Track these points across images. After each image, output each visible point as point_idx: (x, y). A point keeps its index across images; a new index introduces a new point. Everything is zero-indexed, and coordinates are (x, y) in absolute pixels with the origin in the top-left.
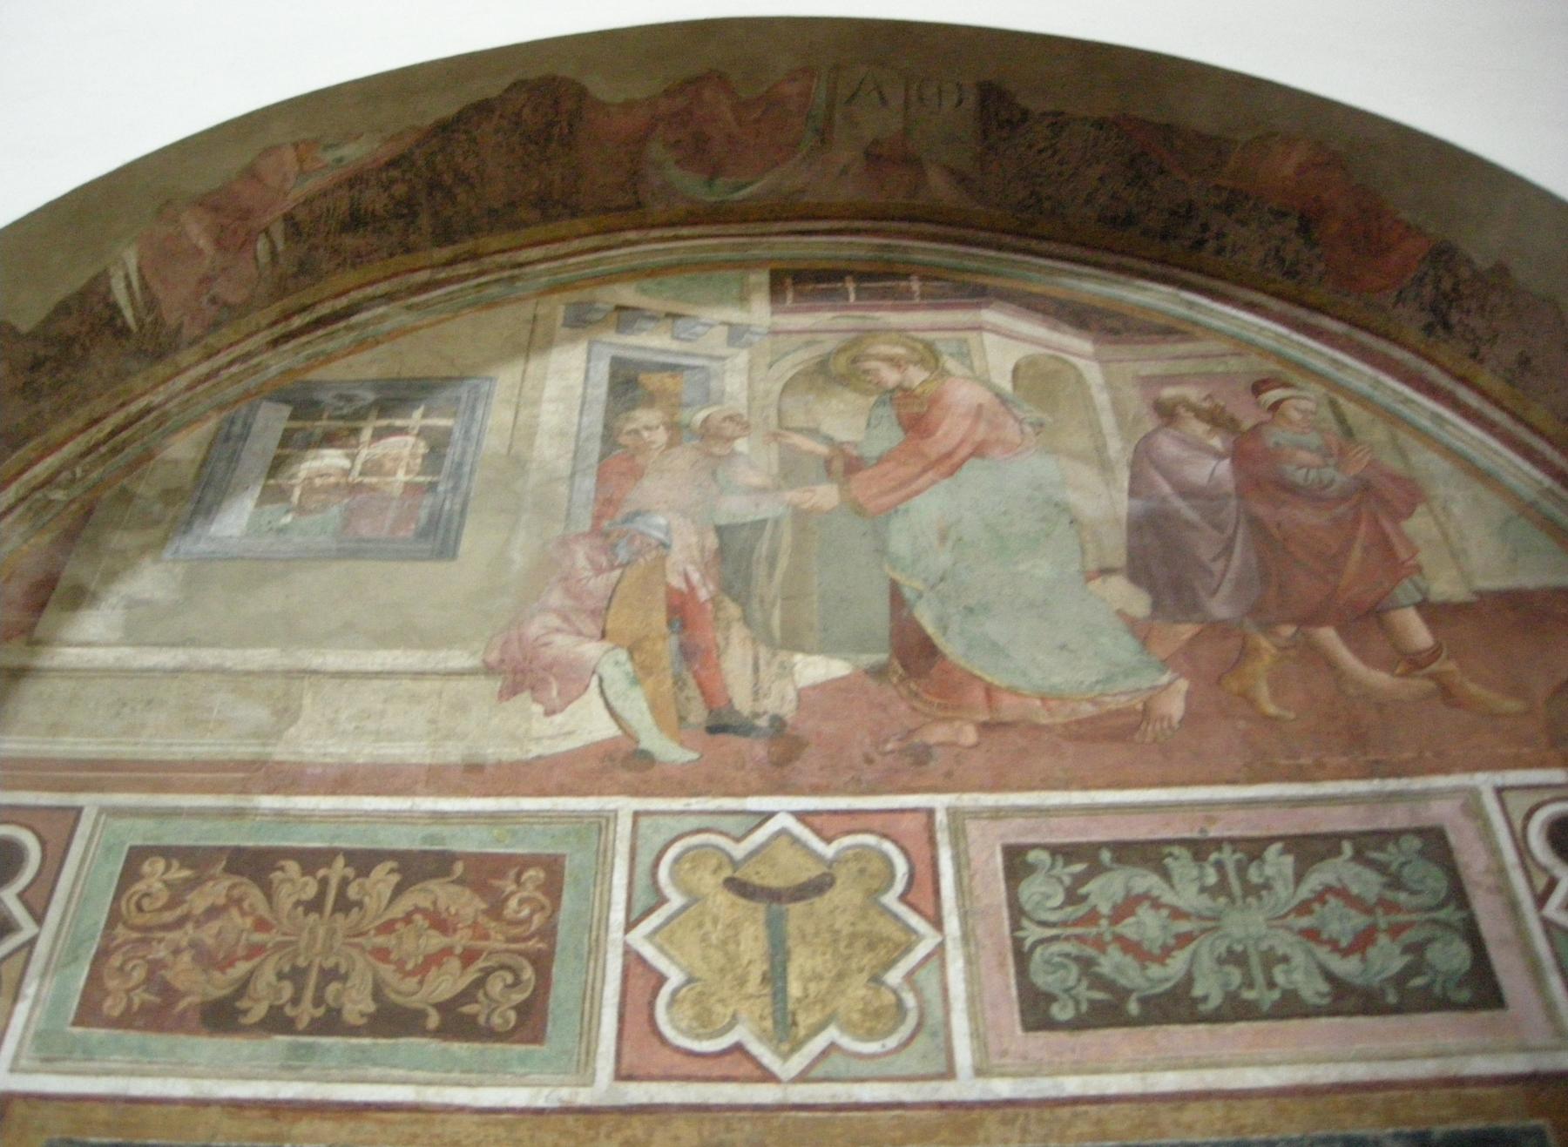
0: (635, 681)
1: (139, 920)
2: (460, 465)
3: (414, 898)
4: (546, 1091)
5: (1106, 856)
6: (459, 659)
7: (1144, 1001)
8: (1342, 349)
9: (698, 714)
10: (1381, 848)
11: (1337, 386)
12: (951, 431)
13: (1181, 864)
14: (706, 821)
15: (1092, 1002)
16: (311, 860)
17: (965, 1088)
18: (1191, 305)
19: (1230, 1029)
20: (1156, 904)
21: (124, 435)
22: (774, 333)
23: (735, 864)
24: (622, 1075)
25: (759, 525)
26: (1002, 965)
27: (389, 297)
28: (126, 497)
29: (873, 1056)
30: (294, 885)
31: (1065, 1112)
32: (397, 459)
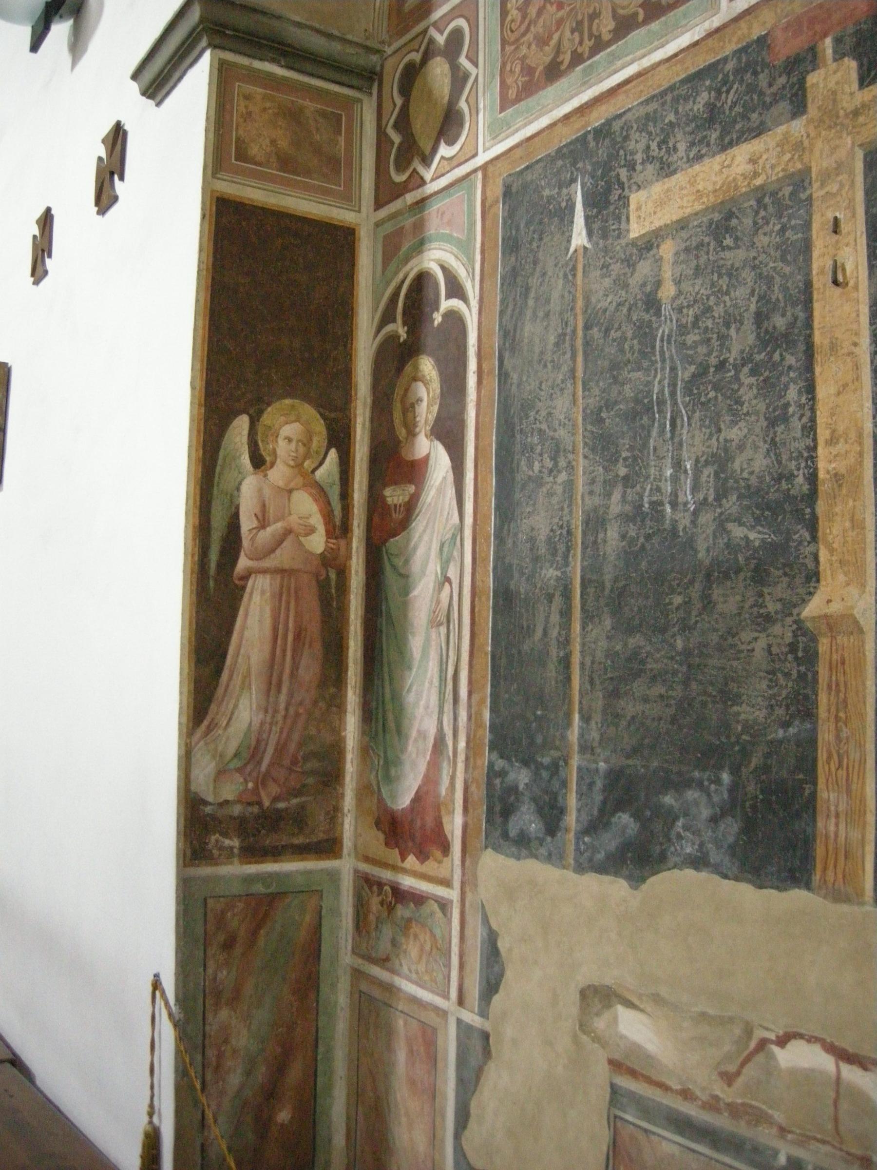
4: (697, 29)
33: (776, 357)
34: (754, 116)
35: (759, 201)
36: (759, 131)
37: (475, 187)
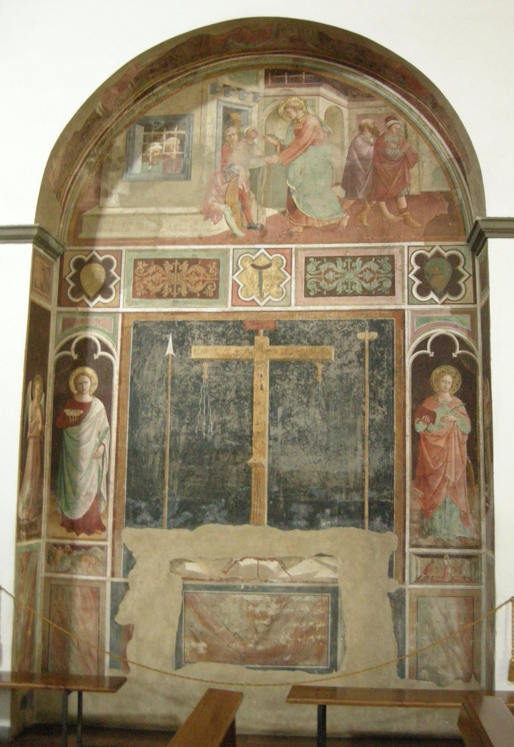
0: (232, 215)
1: (139, 275)
2: (188, 148)
3: (192, 269)
5: (325, 260)
6: (194, 210)
7: (327, 292)
8: (414, 105)
9: (246, 224)
10: (380, 259)
11: (408, 119)
12: (308, 135)
13: (339, 262)
14: (247, 251)
15: (318, 292)
16: (171, 261)
17: (293, 308)
18: (377, 85)
19: (342, 298)
20: (333, 271)
21: (103, 137)
22: (265, 96)
23: (253, 261)
24: (233, 305)
25: (259, 169)
26: (302, 283)
27: (163, 82)
28: (109, 160)
29: (277, 302)
30: (169, 267)
31: (310, 313)
32: (173, 146)
33: (242, 402)
34: (238, 340)
35: (238, 363)
36: (240, 345)
37: (118, 318)
